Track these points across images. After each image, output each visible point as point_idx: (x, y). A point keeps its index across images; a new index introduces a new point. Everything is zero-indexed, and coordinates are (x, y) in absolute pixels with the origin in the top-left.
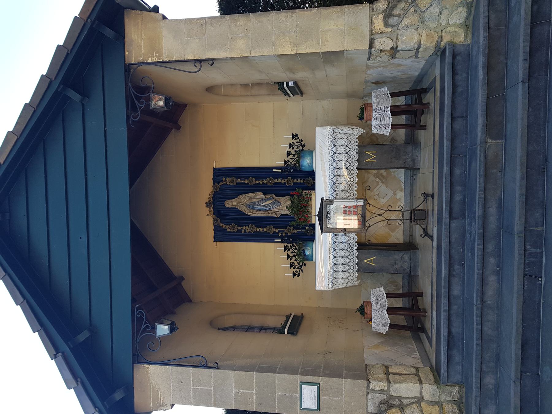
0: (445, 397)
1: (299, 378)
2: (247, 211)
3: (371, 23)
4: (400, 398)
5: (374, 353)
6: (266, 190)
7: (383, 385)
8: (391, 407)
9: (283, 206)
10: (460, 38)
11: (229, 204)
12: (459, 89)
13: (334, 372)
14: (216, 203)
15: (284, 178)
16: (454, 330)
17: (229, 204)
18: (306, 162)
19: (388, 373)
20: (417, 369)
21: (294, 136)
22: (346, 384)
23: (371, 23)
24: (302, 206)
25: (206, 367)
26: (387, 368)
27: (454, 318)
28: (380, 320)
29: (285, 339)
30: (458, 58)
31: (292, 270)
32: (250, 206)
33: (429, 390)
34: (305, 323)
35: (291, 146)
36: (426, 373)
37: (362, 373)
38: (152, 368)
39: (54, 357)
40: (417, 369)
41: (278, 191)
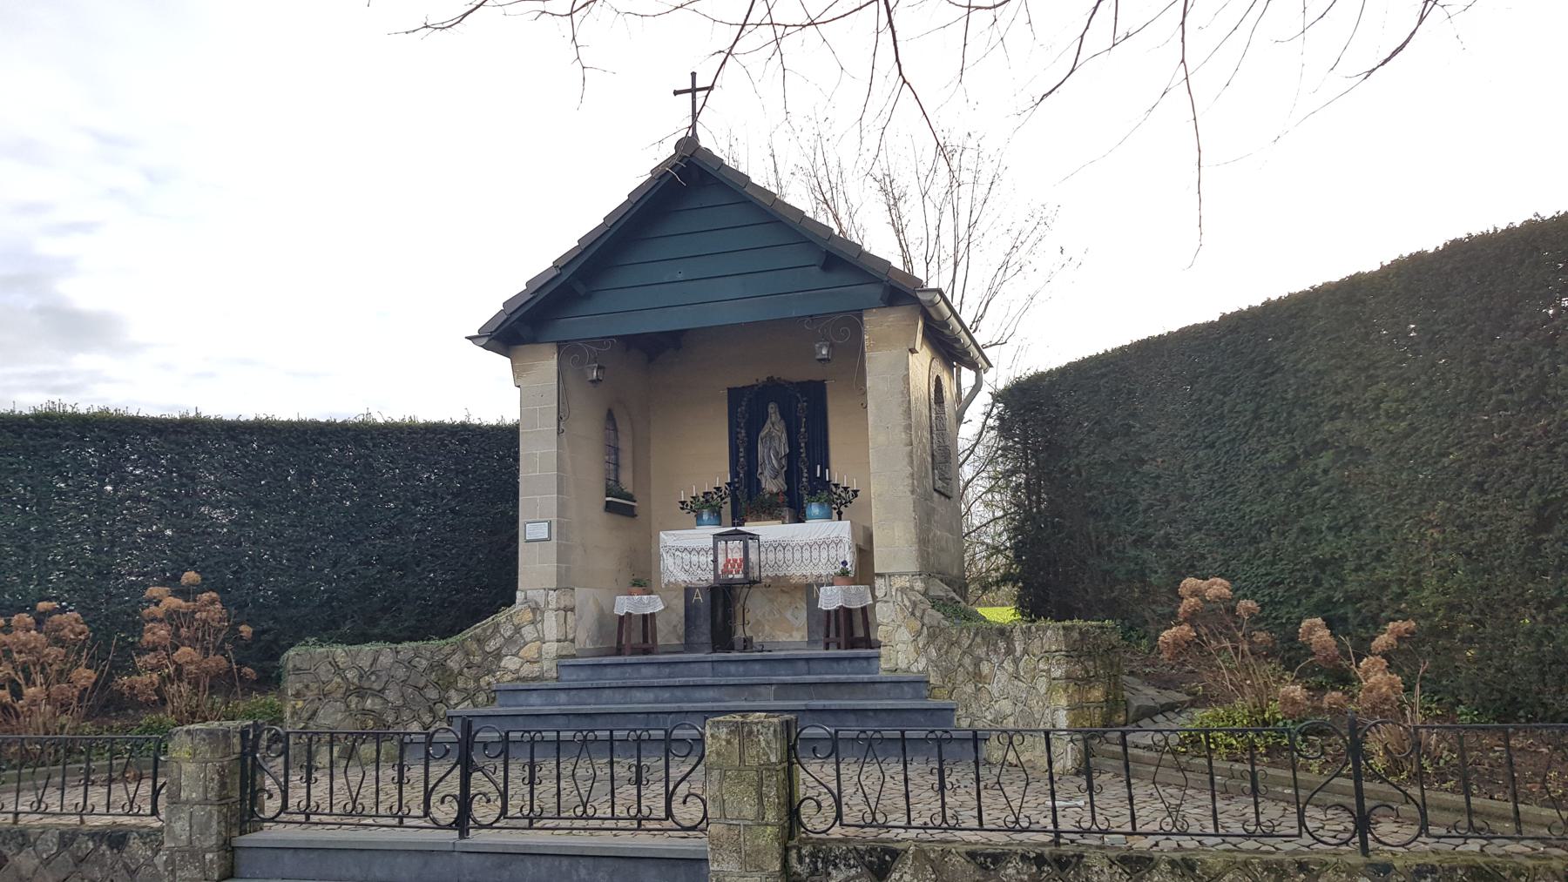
0: (546, 665)
1: (554, 519)
2: (762, 434)
3: (901, 575)
4: (542, 620)
5: (586, 599)
6: (792, 457)
7: (553, 605)
8: (534, 610)
9: (771, 484)
10: (883, 665)
11: (772, 408)
12: (835, 665)
13: (562, 555)
14: (772, 390)
15: (809, 481)
16: (608, 670)
17: (772, 408)
18: (815, 509)
19: (566, 610)
20: (573, 641)
21: (855, 492)
22: (552, 567)
23: (901, 575)
24: (768, 509)
25: (559, 419)
26: (572, 610)
27: (619, 669)
28: (625, 605)
29: (600, 499)
30: (865, 664)
31: (689, 500)
32: (770, 436)
33: (551, 648)
34: (624, 520)
35: (846, 489)
36: (568, 649)
37: (564, 584)
38: (554, 362)
39: (556, 265)
40: (573, 641)
41: (791, 475)
